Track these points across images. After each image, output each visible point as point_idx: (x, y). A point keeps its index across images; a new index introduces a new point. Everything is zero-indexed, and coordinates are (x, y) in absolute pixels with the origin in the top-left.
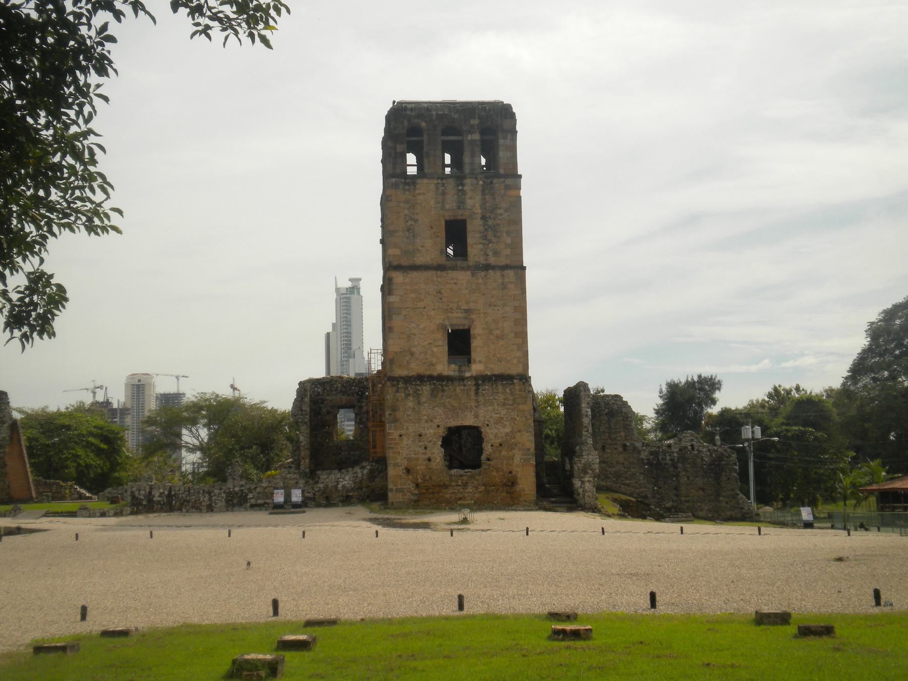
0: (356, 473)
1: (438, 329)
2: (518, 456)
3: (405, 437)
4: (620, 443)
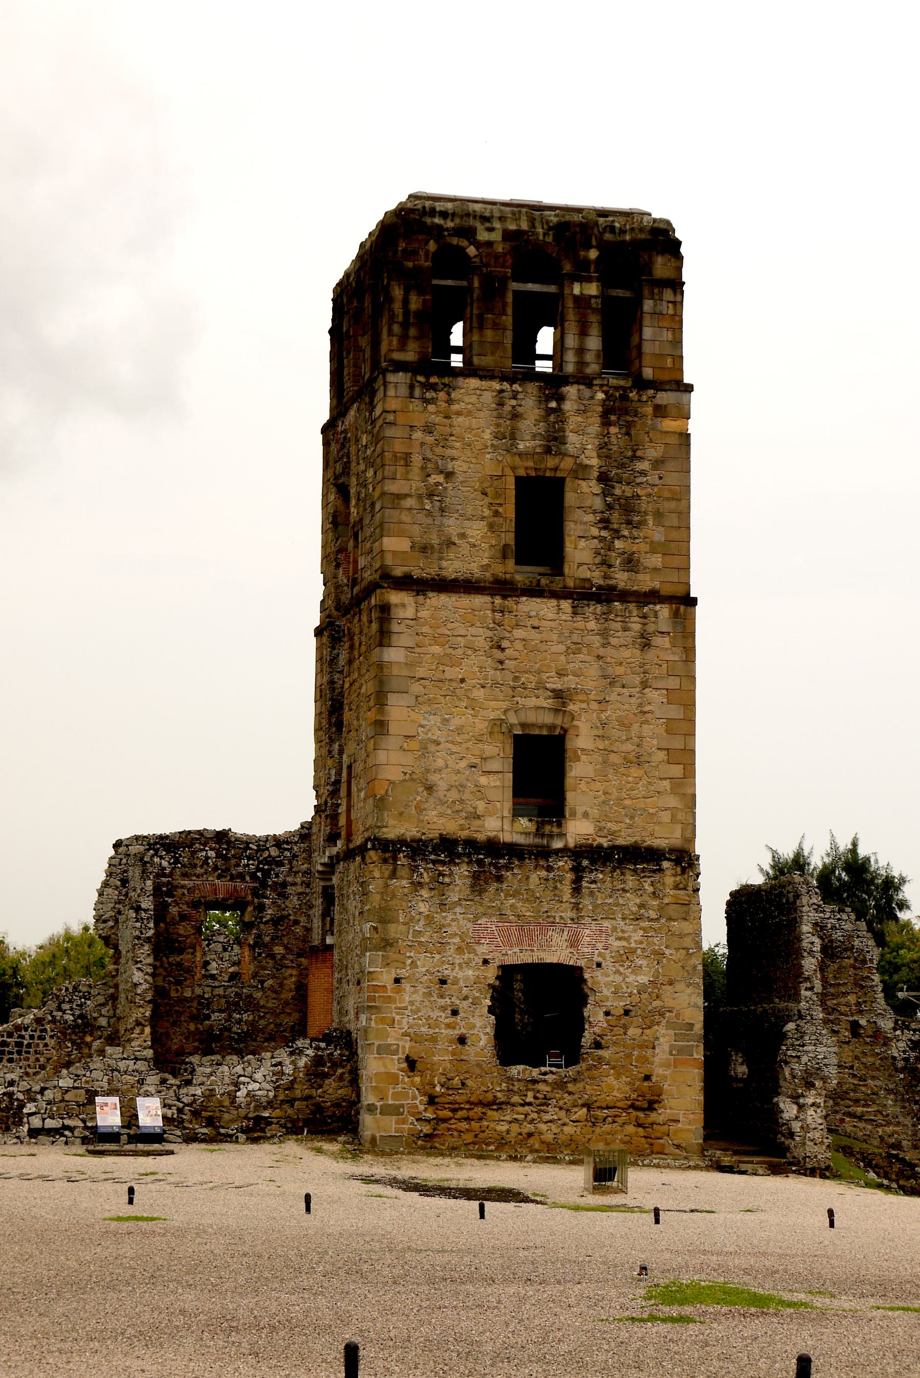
0: (280, 1064)
1: (491, 733)
2: (665, 1038)
3: (408, 985)
4: (845, 1018)
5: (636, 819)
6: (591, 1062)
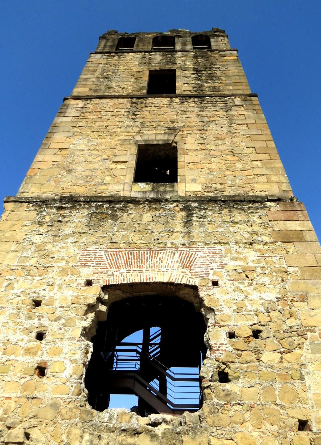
5: (237, 181)
6: (215, 400)
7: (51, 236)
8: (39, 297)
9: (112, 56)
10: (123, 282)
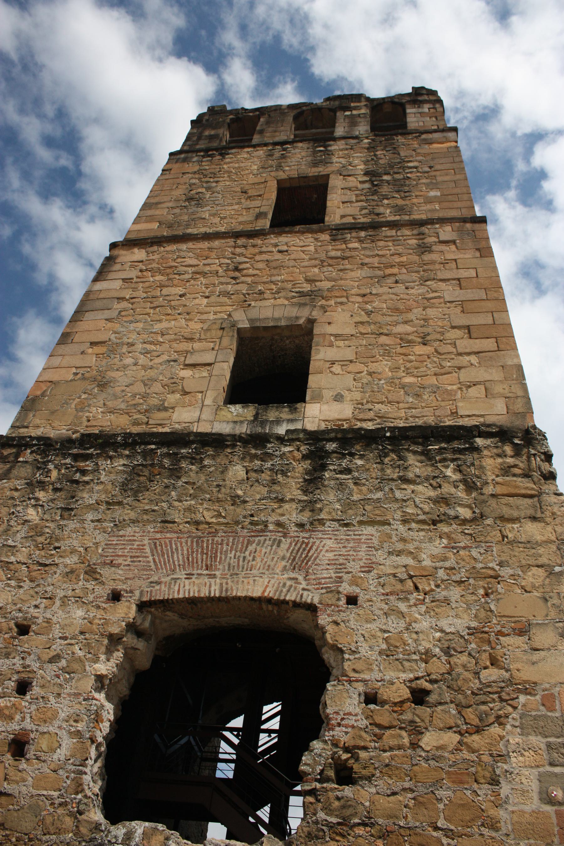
6: (321, 815)
7: (58, 509)
8: (25, 619)
9: (209, 156)
10: (176, 596)
